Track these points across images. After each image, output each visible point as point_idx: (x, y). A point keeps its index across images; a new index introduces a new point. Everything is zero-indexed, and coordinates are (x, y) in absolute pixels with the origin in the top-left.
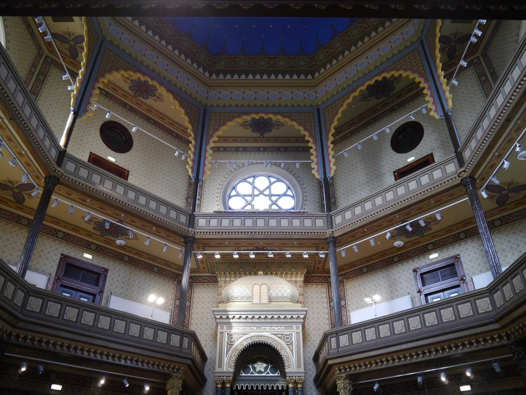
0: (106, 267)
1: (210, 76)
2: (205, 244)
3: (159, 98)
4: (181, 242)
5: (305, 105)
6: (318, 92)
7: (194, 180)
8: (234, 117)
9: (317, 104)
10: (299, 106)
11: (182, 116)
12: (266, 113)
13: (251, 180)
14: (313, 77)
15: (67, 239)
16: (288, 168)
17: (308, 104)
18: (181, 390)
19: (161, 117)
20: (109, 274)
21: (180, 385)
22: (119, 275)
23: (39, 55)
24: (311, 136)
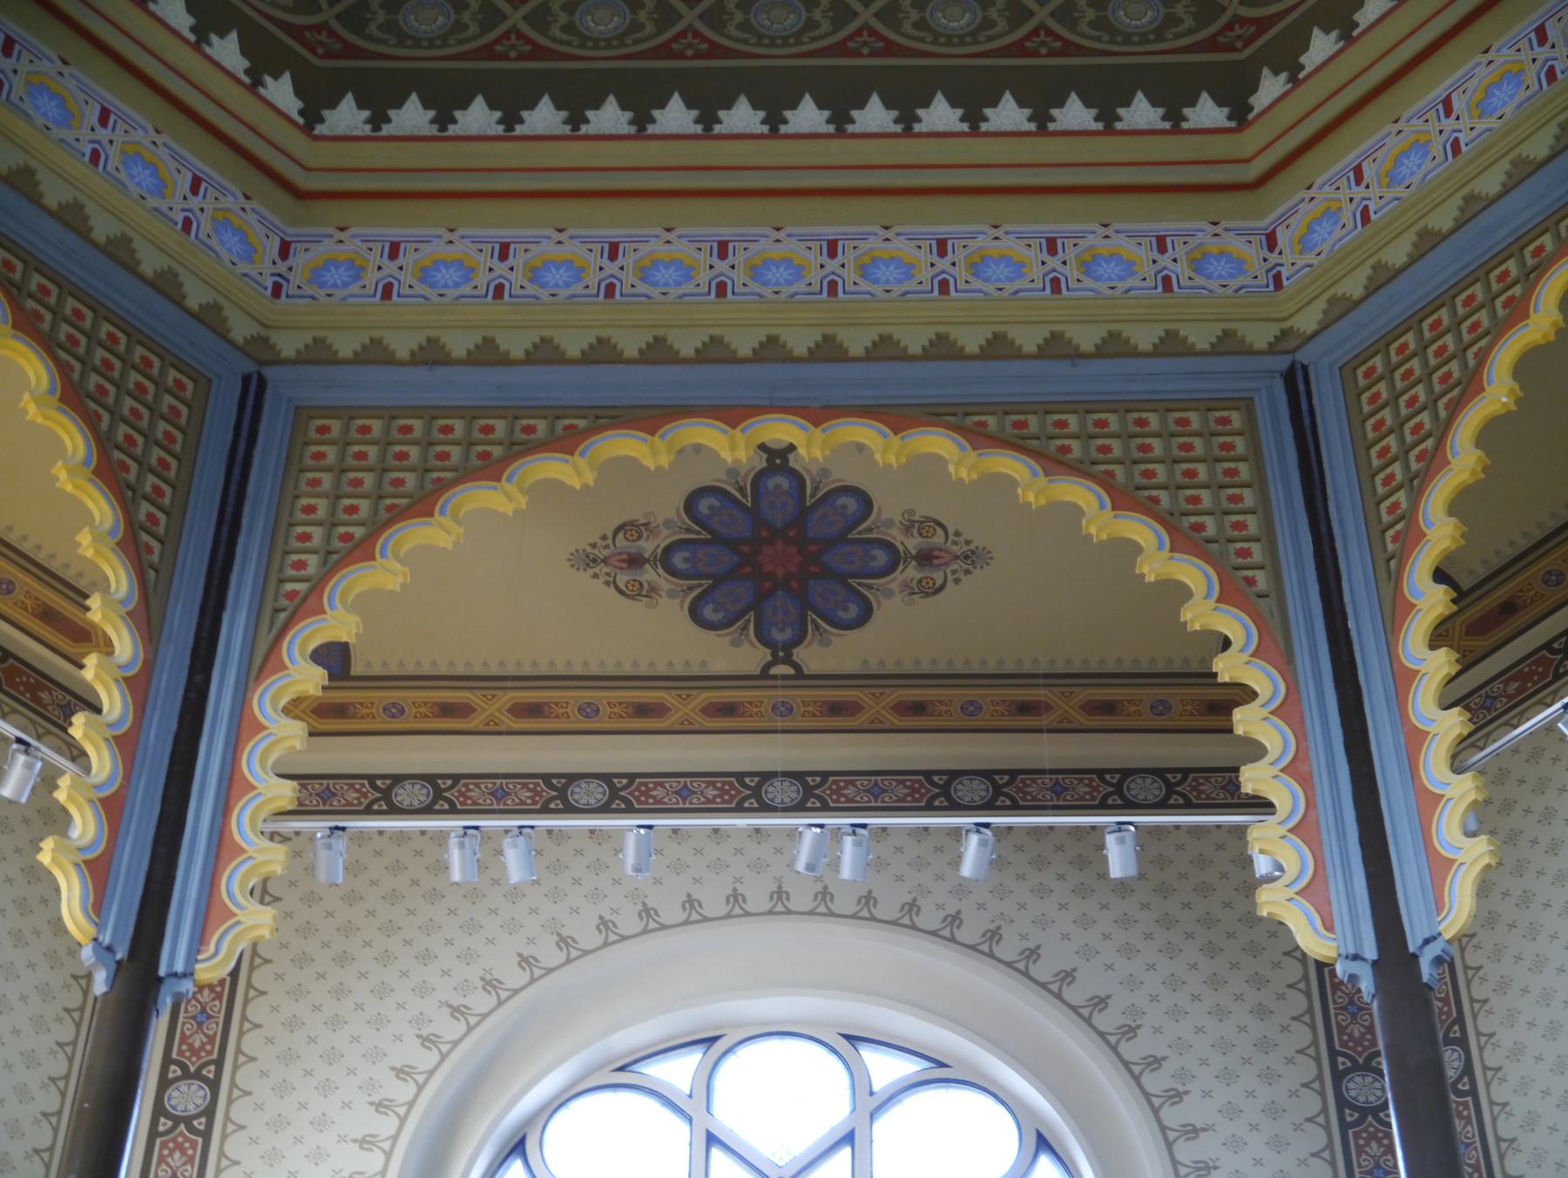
1: (312, 116)
5: (1171, 346)
6: (1282, 237)
7: (113, 982)
8: (521, 448)
9: (1285, 333)
10: (1114, 347)
11: (63, 478)
12: (818, 415)
13: (678, 1072)
14: (1241, 114)
16: (1033, 954)
17: (1200, 336)
24: (1231, 593)
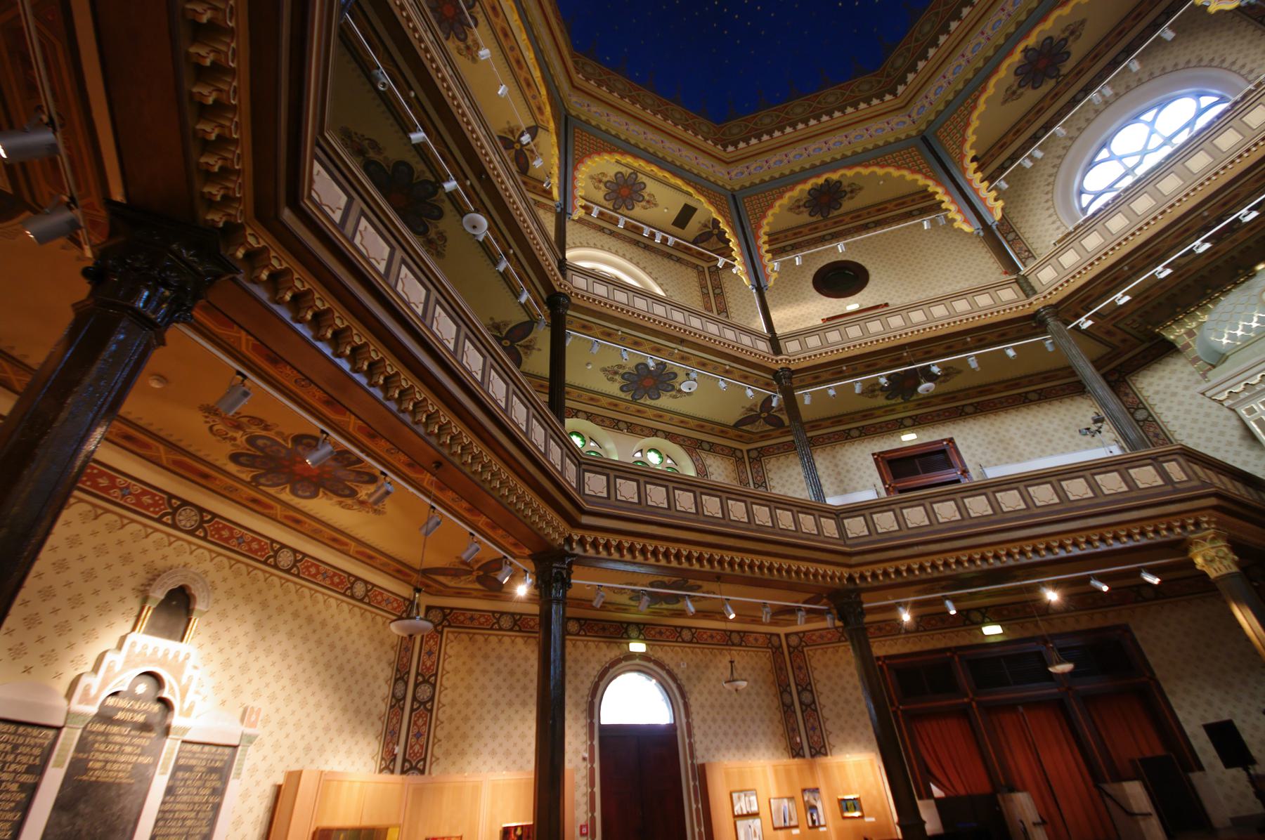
0: (947, 436)
2: (1082, 301)
3: (854, 190)
4: (1035, 328)
13: (1104, 154)
15: (867, 433)
18: (1236, 558)
19: (879, 210)
20: (958, 442)
21: (1225, 549)
22: (975, 437)
23: (701, 273)
